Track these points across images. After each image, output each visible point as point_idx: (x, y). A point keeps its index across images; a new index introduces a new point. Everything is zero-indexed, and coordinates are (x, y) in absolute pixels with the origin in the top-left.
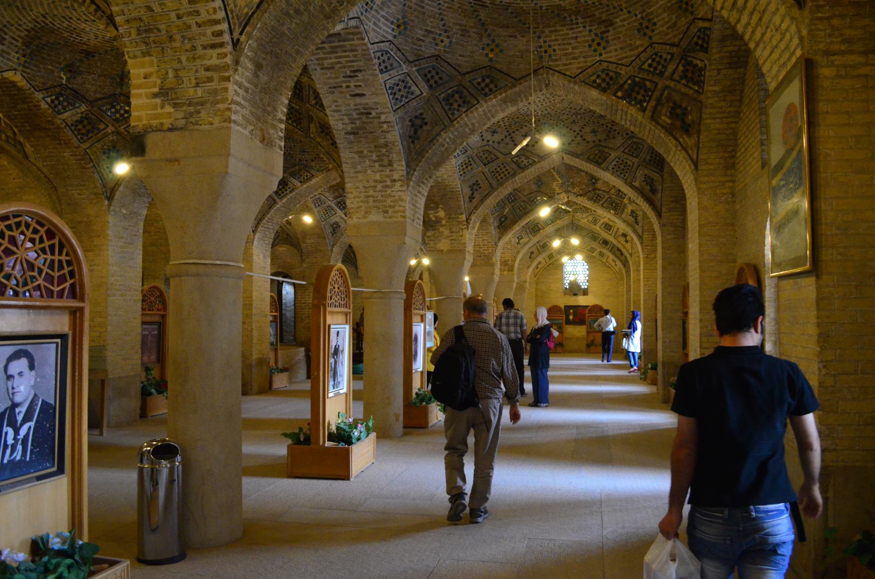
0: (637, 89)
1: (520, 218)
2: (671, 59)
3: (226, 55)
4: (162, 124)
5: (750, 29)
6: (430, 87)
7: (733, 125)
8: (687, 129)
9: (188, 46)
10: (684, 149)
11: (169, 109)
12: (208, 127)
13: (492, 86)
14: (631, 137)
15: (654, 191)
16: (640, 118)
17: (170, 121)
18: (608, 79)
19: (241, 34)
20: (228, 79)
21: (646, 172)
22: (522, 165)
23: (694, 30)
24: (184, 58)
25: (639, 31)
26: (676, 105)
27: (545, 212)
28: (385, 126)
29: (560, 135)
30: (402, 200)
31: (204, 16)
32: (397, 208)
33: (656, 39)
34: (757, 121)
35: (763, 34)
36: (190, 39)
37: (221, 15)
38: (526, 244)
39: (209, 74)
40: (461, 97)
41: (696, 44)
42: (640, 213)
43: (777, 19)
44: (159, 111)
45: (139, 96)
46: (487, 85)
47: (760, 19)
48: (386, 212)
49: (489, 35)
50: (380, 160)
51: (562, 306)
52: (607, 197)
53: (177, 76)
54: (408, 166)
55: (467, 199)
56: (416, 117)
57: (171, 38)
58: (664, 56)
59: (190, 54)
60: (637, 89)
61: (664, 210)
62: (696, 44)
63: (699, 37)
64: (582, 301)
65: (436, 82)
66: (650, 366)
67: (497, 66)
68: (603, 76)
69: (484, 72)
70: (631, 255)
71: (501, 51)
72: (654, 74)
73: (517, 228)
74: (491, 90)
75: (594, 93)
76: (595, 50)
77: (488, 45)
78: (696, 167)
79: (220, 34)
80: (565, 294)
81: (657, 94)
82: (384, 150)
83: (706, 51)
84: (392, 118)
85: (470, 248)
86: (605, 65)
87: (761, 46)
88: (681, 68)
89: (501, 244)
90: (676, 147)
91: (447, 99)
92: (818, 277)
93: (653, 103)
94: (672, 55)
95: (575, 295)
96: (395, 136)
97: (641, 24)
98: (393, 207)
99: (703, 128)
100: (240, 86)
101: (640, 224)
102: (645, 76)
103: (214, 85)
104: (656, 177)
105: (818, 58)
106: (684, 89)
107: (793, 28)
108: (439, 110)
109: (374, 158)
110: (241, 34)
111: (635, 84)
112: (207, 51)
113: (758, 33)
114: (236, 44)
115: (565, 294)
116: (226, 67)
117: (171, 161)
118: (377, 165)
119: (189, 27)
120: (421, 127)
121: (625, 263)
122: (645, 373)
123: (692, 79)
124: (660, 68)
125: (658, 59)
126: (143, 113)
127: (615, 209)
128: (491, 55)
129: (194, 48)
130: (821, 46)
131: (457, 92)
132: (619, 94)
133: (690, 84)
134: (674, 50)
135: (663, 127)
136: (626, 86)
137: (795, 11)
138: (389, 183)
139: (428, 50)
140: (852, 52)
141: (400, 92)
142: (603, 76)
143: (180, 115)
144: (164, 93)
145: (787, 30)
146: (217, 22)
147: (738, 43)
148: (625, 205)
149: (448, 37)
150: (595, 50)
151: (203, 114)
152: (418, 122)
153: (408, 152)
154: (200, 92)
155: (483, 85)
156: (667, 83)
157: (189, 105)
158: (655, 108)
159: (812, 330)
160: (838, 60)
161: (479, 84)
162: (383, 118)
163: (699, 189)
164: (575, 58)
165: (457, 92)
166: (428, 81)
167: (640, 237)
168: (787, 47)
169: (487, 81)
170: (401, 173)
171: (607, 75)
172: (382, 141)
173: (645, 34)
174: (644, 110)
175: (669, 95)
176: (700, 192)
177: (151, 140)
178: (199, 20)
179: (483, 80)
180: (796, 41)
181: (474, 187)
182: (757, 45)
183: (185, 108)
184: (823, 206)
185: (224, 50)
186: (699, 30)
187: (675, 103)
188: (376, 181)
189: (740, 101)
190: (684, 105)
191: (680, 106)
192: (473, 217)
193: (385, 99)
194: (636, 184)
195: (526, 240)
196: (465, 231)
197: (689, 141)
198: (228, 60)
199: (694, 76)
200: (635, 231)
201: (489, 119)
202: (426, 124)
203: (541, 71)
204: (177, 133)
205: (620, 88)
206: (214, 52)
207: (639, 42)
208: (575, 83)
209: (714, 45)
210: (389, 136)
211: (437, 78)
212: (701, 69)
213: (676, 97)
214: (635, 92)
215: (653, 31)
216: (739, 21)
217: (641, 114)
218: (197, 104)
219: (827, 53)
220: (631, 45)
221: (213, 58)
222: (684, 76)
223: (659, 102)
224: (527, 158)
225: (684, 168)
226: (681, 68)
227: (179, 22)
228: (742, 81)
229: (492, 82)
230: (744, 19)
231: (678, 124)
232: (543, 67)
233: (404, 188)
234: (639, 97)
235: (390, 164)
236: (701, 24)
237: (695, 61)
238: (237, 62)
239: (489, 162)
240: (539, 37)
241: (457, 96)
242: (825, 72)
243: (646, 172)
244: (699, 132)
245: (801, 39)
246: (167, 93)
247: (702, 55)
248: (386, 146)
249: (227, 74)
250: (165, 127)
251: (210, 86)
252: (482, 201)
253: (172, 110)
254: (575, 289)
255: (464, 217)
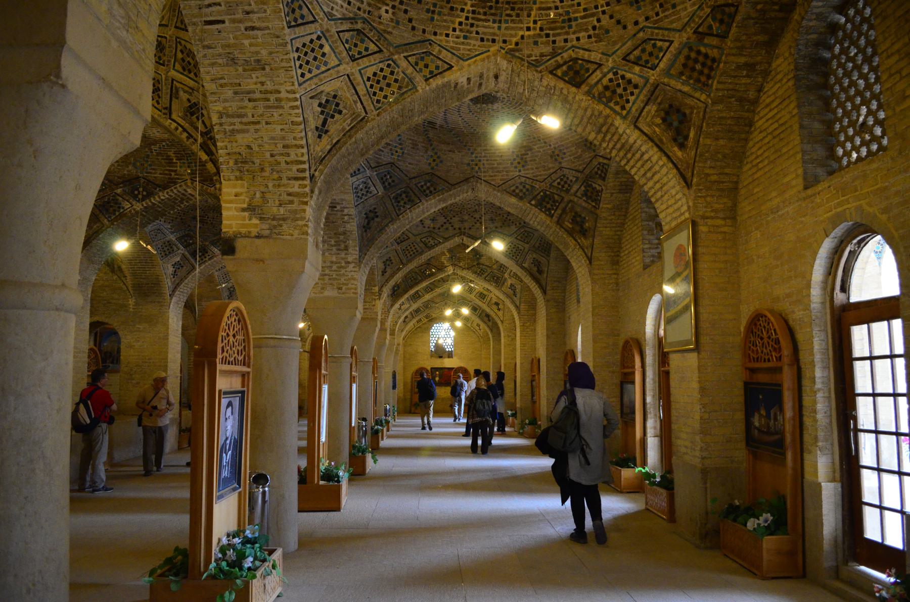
0: (547, 199)
1: (411, 287)
2: (576, 181)
3: (306, 186)
4: (250, 232)
5: (653, 191)
6: (385, 188)
7: (619, 233)
8: (584, 233)
9: (275, 176)
10: (582, 248)
11: (255, 221)
12: (289, 237)
13: (432, 189)
14: (523, 227)
15: (540, 272)
16: (548, 222)
17: (256, 230)
18: (524, 190)
19: (315, 170)
20: (306, 203)
21: (534, 256)
22: (429, 245)
23: (595, 163)
24: (270, 185)
25: (551, 157)
26: (577, 215)
27: (457, 289)
28: (346, 218)
29: (503, 239)
30: (354, 279)
31: (293, 157)
32: (350, 286)
33: (564, 165)
34: (640, 234)
35: (662, 196)
36: (278, 172)
37: (305, 158)
38: (408, 309)
39: (290, 198)
40: (407, 197)
41: (597, 173)
42: (518, 287)
43: (673, 192)
44: (247, 222)
45: (229, 209)
46: (428, 188)
47: (662, 188)
48: (340, 289)
49: (433, 149)
50: (337, 244)
51: (429, 368)
52: (489, 271)
53: (263, 197)
54: (360, 250)
55: (380, 273)
56: (370, 211)
57: (262, 170)
58: (571, 178)
59: (276, 183)
60: (547, 199)
61: (548, 288)
62: (597, 173)
63: (598, 169)
64: (448, 363)
65: (389, 184)
66: (527, 421)
67: (437, 173)
68: (521, 187)
69: (428, 178)
70: (502, 322)
71: (441, 162)
72: (561, 190)
73: (406, 296)
74: (431, 192)
75: (513, 200)
76: (516, 167)
77: (432, 156)
78: (590, 262)
79: (303, 171)
80: (432, 356)
81: (563, 205)
82: (342, 237)
83: (604, 179)
84: (353, 211)
85: (379, 317)
86: (523, 179)
87: (660, 202)
88: (583, 188)
89: (392, 311)
90: (575, 245)
91: (396, 198)
92: (698, 353)
93: (559, 211)
94: (577, 178)
95: (441, 357)
96: (353, 227)
97: (553, 152)
98: (347, 284)
99: (596, 233)
100: (311, 206)
101: (518, 296)
102: (555, 191)
103: (294, 206)
104: (543, 260)
105: (698, 220)
106: (584, 204)
107: (684, 200)
108: (390, 206)
109: (333, 243)
110: (315, 170)
111: (546, 195)
112: (291, 182)
113: (659, 194)
114: (312, 177)
115: (432, 356)
116: (304, 195)
117: (257, 260)
118: (334, 248)
119: (280, 163)
120: (373, 219)
121: (494, 328)
122: (523, 428)
123: (591, 197)
124: (566, 186)
125: (565, 179)
126: (234, 223)
127: (496, 282)
128: (433, 164)
129: (280, 178)
130: (701, 213)
131: (404, 192)
132: (533, 202)
133: (590, 201)
134: (579, 175)
135: (566, 230)
136: (539, 197)
137: (686, 190)
138: (343, 264)
139: (386, 158)
140: (717, 218)
141: (361, 193)
142: (521, 187)
143: (266, 226)
144: (251, 209)
145: (679, 200)
146: (304, 163)
147: (627, 176)
148: (506, 279)
149: (401, 149)
150: (516, 167)
151: (285, 227)
152: (371, 215)
153: (362, 238)
154: (282, 210)
155: (425, 187)
156: (572, 198)
157: (274, 219)
158: (561, 215)
159: (695, 385)
160: (710, 222)
161: (422, 186)
162: (346, 211)
163: (592, 279)
164: (498, 172)
165: (404, 192)
166: (384, 183)
167: (517, 307)
168: (678, 209)
169: (428, 184)
170: (355, 256)
171: (524, 187)
172: (341, 230)
173: (556, 160)
174: (552, 216)
175: (573, 207)
176: (594, 282)
177: (240, 244)
178: (288, 159)
179: (425, 184)
180: (685, 208)
181: (387, 262)
182: (657, 201)
183: (269, 221)
184: (701, 310)
185: (305, 182)
186: (599, 164)
187: (576, 213)
188: (332, 262)
189: (625, 216)
190: (583, 215)
191: (580, 216)
192: (384, 289)
193: (350, 197)
194: (525, 265)
195: (407, 306)
196: (377, 301)
197: (586, 242)
198: (307, 190)
199: (593, 195)
200: (513, 302)
201: (424, 213)
202: (377, 217)
203: (472, 180)
204: (262, 240)
205: (534, 198)
206: (297, 183)
207: (550, 165)
208: (498, 191)
209: (610, 176)
210: (348, 226)
211: (390, 181)
212: (598, 191)
213: (578, 209)
214: (545, 202)
215: (563, 158)
216: (645, 184)
217: (549, 219)
218: (280, 219)
219: (704, 217)
220: (544, 166)
221: (295, 187)
222: (585, 194)
223: (564, 210)
224: (434, 239)
225: (580, 261)
226: (583, 188)
227: (272, 159)
228: (628, 202)
229: (432, 185)
230: (650, 184)
231: (578, 228)
232: (473, 177)
233: (357, 269)
234: (549, 206)
235: (346, 248)
236: (601, 160)
237: (594, 185)
238: (312, 191)
239: (402, 242)
240: (472, 153)
241: (404, 195)
242: (703, 229)
243: (534, 256)
244: (594, 237)
245: (689, 207)
246: (254, 210)
247: (600, 182)
248: (345, 233)
249: (305, 200)
250: (253, 235)
251: (289, 207)
252: (392, 276)
253: (258, 222)
254: (440, 352)
255: (377, 289)
